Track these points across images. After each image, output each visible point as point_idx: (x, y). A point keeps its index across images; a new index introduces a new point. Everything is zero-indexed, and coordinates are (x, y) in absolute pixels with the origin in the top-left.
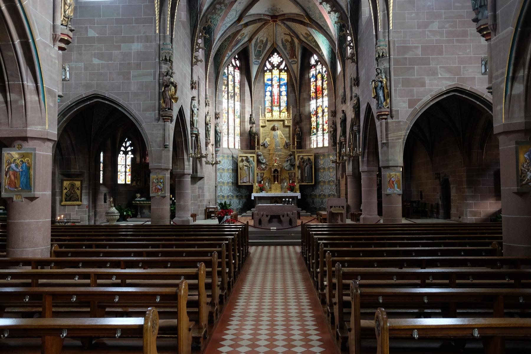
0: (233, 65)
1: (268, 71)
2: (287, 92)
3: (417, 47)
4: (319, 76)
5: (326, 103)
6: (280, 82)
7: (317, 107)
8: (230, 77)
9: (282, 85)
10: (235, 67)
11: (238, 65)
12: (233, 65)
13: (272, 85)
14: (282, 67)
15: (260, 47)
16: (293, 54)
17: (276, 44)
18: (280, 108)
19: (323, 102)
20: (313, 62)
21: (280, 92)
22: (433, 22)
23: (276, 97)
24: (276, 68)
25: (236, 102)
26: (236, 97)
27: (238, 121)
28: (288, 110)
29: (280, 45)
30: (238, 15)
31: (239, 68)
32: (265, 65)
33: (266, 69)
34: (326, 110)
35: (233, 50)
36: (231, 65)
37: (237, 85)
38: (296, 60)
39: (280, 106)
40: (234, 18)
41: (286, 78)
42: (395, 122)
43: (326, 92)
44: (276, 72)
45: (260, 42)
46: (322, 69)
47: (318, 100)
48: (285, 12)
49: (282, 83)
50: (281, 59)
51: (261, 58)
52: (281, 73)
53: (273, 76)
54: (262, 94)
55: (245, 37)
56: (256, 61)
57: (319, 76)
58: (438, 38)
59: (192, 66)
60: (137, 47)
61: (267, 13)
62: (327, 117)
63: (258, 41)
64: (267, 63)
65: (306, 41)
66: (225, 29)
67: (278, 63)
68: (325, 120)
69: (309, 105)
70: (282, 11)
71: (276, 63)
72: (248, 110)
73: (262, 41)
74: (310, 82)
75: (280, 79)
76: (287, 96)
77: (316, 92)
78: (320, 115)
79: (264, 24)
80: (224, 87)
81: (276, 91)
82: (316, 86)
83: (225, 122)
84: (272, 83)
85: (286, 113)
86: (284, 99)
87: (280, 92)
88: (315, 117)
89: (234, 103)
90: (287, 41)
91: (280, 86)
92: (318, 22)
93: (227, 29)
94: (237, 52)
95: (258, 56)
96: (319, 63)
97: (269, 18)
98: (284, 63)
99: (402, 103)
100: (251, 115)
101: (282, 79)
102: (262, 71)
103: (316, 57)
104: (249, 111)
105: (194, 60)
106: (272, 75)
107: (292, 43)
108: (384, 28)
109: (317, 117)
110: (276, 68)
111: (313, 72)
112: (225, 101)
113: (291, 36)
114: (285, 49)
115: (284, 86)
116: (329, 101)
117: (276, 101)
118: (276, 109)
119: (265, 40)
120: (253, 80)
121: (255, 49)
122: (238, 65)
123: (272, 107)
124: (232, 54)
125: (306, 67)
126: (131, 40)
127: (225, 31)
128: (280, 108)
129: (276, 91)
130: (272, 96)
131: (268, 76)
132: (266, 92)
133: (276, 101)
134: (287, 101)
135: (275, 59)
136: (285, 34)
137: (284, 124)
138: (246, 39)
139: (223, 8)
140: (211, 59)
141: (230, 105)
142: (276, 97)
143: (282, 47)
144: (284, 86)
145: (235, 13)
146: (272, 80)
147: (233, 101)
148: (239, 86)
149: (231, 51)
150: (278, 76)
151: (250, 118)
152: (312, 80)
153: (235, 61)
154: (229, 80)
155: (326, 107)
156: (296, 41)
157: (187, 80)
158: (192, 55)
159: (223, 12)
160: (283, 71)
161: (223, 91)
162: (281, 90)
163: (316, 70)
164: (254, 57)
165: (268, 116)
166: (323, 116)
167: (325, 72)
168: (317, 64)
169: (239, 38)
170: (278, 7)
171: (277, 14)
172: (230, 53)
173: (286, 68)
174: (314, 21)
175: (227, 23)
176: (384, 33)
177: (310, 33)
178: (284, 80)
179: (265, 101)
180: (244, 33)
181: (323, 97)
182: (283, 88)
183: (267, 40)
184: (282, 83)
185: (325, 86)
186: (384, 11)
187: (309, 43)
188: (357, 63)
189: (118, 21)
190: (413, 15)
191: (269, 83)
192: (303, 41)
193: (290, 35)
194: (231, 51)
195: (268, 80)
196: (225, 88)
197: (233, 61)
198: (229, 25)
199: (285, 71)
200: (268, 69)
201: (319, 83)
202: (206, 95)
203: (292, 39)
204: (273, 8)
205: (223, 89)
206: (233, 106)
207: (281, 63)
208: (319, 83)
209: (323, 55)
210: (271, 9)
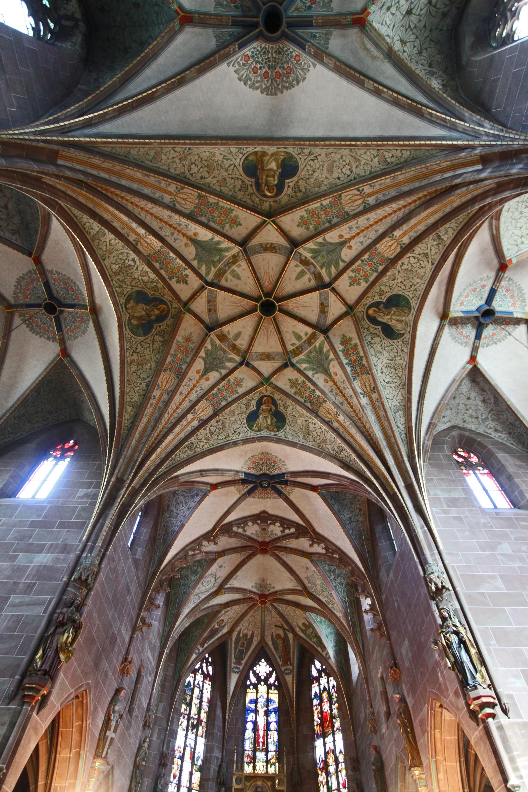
0: (203, 673)
1: (251, 687)
2: (279, 723)
3: (494, 577)
4: (325, 695)
5: (340, 746)
6: (267, 706)
7: (326, 753)
8: (197, 691)
9: (271, 712)
10: (206, 676)
11: (211, 673)
12: (203, 673)
13: (256, 712)
14: (272, 680)
15: (243, 644)
16: (287, 660)
17: (264, 640)
18: (267, 755)
19: (334, 741)
20: (315, 673)
21: (268, 723)
22: (501, 543)
23: (261, 733)
24: (262, 683)
25: (199, 738)
26: (200, 728)
27: (197, 776)
28: (279, 759)
29: (270, 643)
30: (217, 585)
31: (212, 679)
32: (249, 678)
33: (248, 683)
34: (341, 758)
35: (206, 645)
36: (200, 672)
37: (205, 706)
38: (290, 667)
39: (267, 751)
40: (211, 588)
41: (277, 700)
42: (518, 724)
43: (337, 724)
44: (263, 688)
45: (243, 636)
46: (328, 682)
47: (326, 739)
48: (277, 589)
49: (271, 708)
50: (271, 669)
51: (243, 662)
52: (270, 691)
53: (259, 695)
54: (239, 725)
55: (224, 627)
56: (236, 668)
57: (325, 695)
58: (520, 565)
59: (134, 631)
60: (43, 559)
61: (254, 590)
62: (344, 772)
63: (241, 635)
64: (251, 674)
65: (305, 637)
66: (198, 601)
67: (265, 675)
68: (341, 782)
69: (313, 748)
70: (274, 588)
71: (263, 675)
72: (217, 754)
73: (245, 635)
74: (312, 706)
75: (268, 701)
76: (279, 731)
77: (322, 725)
78: (332, 769)
79: (250, 608)
80: (184, 706)
81: (261, 721)
82: (322, 712)
83: (175, 777)
84: (256, 706)
85: (277, 764)
86: (274, 736)
87: (268, 723)
88: (324, 774)
89: (196, 738)
90: (278, 636)
91: (267, 713)
92: (321, 597)
93: (200, 602)
94: (210, 649)
95: (239, 660)
96: (323, 675)
97: (257, 598)
98: (274, 675)
99: (512, 680)
100: (220, 766)
101: (271, 700)
102: (243, 687)
103: (318, 664)
104: (217, 758)
105: (139, 623)
106: (257, 693)
107: (285, 640)
108: (431, 550)
109: (328, 774)
110: (262, 683)
111: (315, 689)
112: (181, 733)
113: (284, 630)
114: (276, 649)
115: (273, 713)
116: (345, 738)
117: (261, 740)
118: (260, 755)
119: (250, 633)
120: (229, 699)
121: (236, 648)
122: (211, 673)
123: (255, 751)
124: (203, 651)
125: (305, 681)
126: (40, 549)
127: (197, 605)
128: (267, 755)
129: (261, 721)
130: (255, 730)
131: (251, 695)
132: (247, 722)
133: (261, 740)
134: (279, 740)
135: (263, 668)
136: (276, 626)
137: (273, 785)
138: (225, 630)
139: (199, 570)
140: (169, 644)
141: (189, 742)
142: (261, 733)
143: (272, 647)
144: (273, 713)
145: (213, 580)
146: (256, 701)
147: (194, 736)
148: (207, 709)
149: (202, 645)
150: (265, 696)
151: (219, 771)
152: (315, 702)
153: (207, 666)
154: (195, 695)
155: (341, 752)
156: (290, 636)
157: (116, 650)
158: (139, 615)
159: (198, 575)
160: (273, 688)
161: (180, 714)
162: (270, 720)
163: (319, 685)
164: (234, 660)
165: (248, 769)
166: (337, 771)
167: (333, 687)
168: (320, 676)
169: (216, 626)
170: (268, 582)
171: (267, 593)
172: (201, 649)
173: (276, 683)
174: (315, 596)
175: (202, 593)
176: (432, 555)
177: (309, 623)
178: (274, 702)
179: (243, 740)
180: (223, 620)
181: (333, 733)
182: (273, 717)
183: (252, 635)
184: (271, 708)
185: (335, 711)
186: (422, 528)
187: (308, 640)
188: (389, 639)
189: (33, 524)
190: (467, 533)
191: (252, 706)
192: (300, 637)
193: (282, 627)
194: (202, 645)
195: (251, 702)
196: (186, 710)
197: (204, 665)
198: (203, 597)
199: (276, 688)
200: (251, 684)
201: (326, 707)
202: (149, 704)
203: (285, 634)
204: (262, 584)
205: (183, 710)
206: (193, 746)
207: (269, 675)
208: (326, 707)
209: (330, 657)
210: (260, 584)
